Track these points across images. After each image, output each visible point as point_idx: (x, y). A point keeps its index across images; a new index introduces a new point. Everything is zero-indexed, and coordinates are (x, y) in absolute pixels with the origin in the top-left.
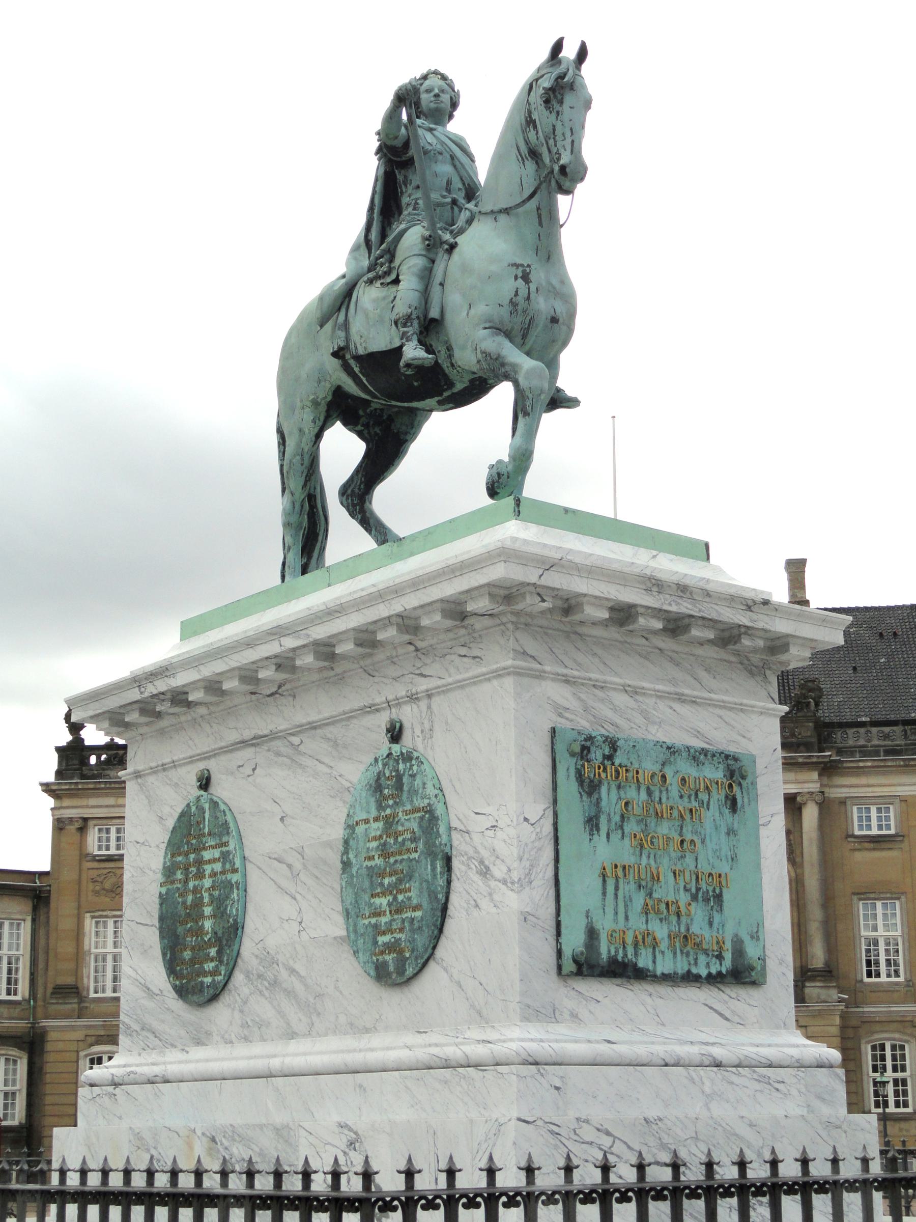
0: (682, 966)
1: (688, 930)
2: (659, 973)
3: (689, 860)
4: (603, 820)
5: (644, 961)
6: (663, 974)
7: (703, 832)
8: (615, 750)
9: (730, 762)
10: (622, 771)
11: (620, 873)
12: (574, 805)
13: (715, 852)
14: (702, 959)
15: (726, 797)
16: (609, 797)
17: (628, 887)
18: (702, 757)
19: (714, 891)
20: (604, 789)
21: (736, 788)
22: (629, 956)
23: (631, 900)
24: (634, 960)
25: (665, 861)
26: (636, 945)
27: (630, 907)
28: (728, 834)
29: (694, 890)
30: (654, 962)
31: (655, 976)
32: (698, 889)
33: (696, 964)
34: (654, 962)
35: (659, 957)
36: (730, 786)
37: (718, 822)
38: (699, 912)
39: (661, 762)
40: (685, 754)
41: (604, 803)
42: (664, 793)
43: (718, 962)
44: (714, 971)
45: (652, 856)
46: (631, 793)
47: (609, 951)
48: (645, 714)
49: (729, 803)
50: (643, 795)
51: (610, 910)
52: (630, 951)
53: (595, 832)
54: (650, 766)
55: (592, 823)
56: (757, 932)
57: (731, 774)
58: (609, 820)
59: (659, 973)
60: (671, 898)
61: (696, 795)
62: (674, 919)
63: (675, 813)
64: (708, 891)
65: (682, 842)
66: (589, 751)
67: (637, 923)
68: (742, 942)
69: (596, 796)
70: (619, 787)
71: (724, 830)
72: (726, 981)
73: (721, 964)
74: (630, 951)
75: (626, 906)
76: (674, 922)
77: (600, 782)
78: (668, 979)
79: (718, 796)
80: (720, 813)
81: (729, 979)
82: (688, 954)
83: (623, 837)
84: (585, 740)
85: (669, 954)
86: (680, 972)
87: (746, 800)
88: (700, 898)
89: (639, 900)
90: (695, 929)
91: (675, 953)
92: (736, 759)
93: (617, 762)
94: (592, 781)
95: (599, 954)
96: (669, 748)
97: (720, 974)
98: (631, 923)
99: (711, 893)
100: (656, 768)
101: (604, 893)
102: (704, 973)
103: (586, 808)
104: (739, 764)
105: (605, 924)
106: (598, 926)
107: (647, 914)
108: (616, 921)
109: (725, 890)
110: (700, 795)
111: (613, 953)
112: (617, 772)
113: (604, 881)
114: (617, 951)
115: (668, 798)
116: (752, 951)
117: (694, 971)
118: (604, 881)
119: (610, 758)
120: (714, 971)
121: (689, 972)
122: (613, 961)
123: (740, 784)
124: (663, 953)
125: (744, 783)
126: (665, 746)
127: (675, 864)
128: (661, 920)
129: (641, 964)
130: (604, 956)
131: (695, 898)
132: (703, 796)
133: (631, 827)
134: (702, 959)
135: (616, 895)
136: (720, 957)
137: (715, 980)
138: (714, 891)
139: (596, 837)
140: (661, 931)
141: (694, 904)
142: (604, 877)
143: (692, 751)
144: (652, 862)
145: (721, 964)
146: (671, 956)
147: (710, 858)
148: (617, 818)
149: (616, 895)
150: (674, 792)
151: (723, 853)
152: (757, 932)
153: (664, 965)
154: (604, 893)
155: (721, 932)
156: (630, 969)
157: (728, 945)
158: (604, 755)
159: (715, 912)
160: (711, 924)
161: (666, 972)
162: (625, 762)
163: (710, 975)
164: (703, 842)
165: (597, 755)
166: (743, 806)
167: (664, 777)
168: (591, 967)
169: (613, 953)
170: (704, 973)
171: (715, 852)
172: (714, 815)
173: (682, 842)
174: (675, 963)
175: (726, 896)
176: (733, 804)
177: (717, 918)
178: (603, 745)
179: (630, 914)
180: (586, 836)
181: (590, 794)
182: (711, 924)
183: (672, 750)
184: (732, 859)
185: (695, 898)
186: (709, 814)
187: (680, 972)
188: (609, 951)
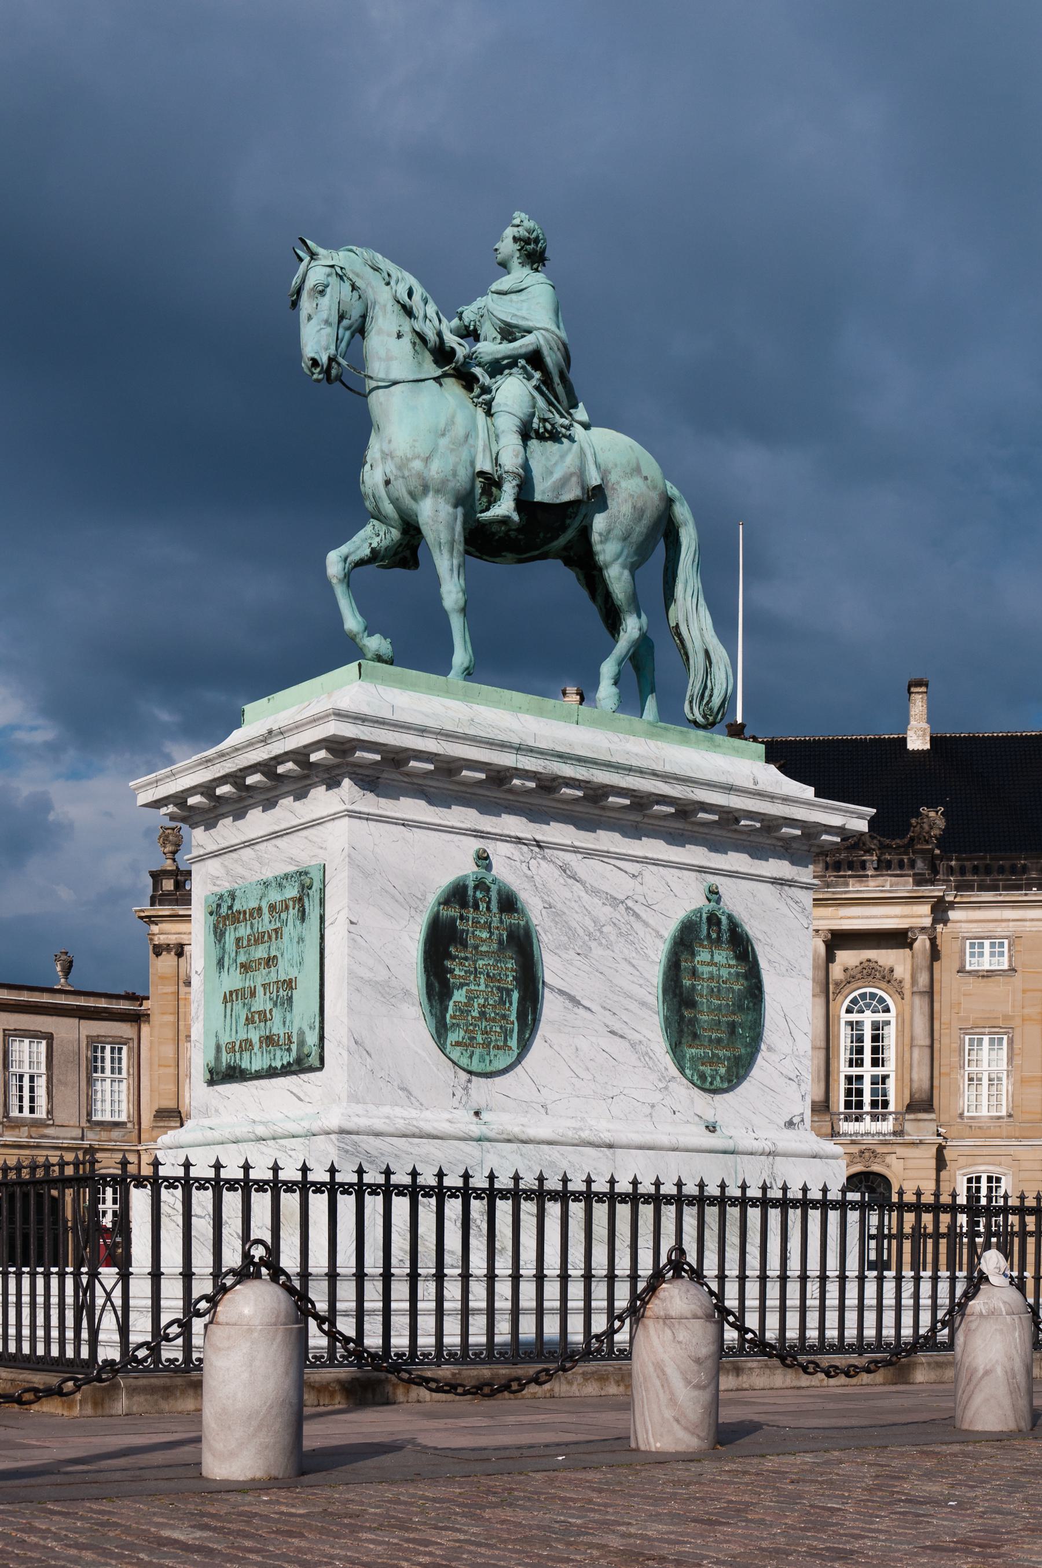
3: (273, 975)
14: (279, 1053)
21: (306, 900)
32: (277, 996)
40: (274, 885)
44: (285, 1063)
48: (259, 860)
57: (305, 888)
97: (289, 1063)
102: (279, 1065)
134: (279, 1053)
136: (289, 1050)
137: (286, 1071)
160: (284, 1023)
167: (260, 909)
170: (279, 1065)
182: (284, 1023)
183: (266, 884)
185: (275, 1005)
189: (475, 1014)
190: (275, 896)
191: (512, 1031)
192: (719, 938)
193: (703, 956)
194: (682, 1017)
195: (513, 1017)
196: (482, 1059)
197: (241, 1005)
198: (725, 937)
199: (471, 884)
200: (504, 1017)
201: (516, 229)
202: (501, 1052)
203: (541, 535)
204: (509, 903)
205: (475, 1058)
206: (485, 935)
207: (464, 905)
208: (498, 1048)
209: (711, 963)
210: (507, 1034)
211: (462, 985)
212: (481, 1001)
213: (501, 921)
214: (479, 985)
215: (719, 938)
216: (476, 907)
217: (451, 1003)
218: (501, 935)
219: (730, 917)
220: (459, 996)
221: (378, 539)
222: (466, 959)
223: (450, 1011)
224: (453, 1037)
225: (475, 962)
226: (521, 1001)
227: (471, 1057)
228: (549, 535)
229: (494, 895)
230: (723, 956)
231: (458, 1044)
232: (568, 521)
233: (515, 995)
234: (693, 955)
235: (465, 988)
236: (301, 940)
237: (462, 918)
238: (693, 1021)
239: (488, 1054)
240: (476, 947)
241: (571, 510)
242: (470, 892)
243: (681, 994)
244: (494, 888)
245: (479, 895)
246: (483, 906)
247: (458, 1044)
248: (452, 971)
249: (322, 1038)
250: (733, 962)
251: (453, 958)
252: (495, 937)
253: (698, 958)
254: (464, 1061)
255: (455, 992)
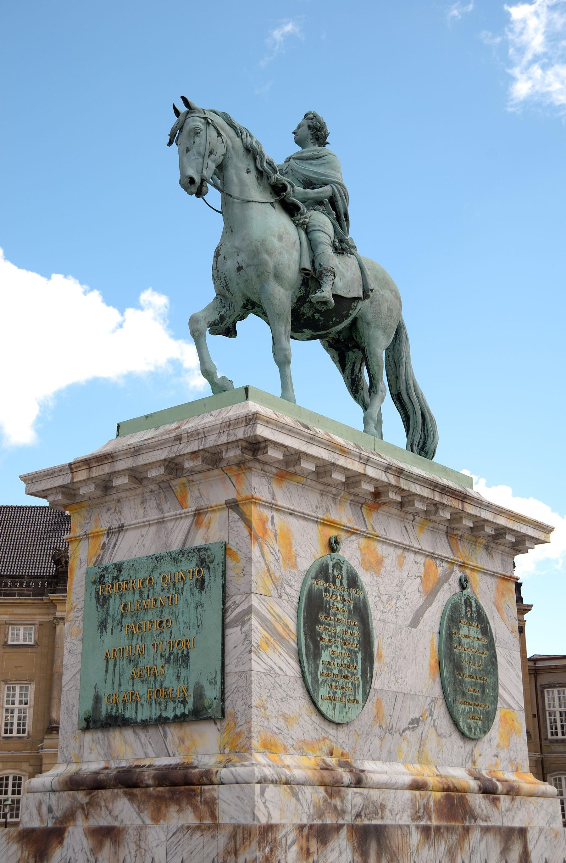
0: (155, 713)
1: (162, 685)
2: (139, 720)
3: (166, 635)
4: (110, 621)
5: (129, 713)
6: (142, 720)
7: (177, 612)
8: (121, 571)
9: (201, 553)
10: (124, 585)
11: (118, 655)
12: (95, 616)
13: (185, 623)
14: (171, 705)
15: (197, 580)
16: (115, 606)
17: (122, 663)
18: (181, 556)
19: (183, 653)
20: (112, 600)
22: (120, 711)
23: (124, 672)
24: (123, 713)
25: (148, 640)
26: (124, 702)
27: (122, 677)
28: (196, 608)
29: (167, 655)
30: (136, 713)
31: (136, 723)
32: (170, 654)
33: (166, 709)
34: (136, 713)
35: (140, 708)
36: (199, 571)
37: (189, 601)
38: (170, 671)
39: (150, 569)
41: (111, 610)
42: (151, 591)
43: (182, 706)
44: (179, 713)
45: (140, 638)
46: (129, 598)
47: (107, 709)
49: (198, 584)
50: (137, 596)
51: (109, 682)
52: (121, 706)
53: (104, 630)
54: (143, 575)
55: (103, 625)
56: (215, 678)
57: (202, 562)
58: (113, 621)
59: (139, 720)
60: (151, 665)
61: (174, 585)
62: (152, 679)
63: (158, 603)
64: (178, 654)
65: (161, 622)
66: (104, 578)
67: (127, 687)
68: (202, 687)
69: (106, 606)
70: (121, 596)
71: (193, 605)
72: (188, 719)
73: (185, 707)
74: (121, 706)
75: (120, 676)
76: (152, 682)
77: (110, 596)
78: (145, 724)
79: (190, 581)
80: (191, 593)
81: (191, 717)
82: (160, 704)
83: (121, 630)
84: (103, 571)
85: (147, 706)
86: (154, 717)
87: (212, 578)
88: (172, 661)
89: (129, 670)
90: (166, 684)
91: (151, 704)
92: (206, 550)
93: (121, 580)
94: (105, 597)
95: (100, 712)
96: (157, 558)
97: (183, 714)
98: (122, 687)
99: (180, 655)
100: (146, 575)
101: (107, 671)
102: (171, 715)
103: (100, 616)
104: (209, 553)
105: (105, 691)
106: (101, 694)
107: (133, 679)
108: (113, 688)
109: (190, 651)
110: (177, 585)
111: (109, 711)
112: (119, 585)
113: (107, 662)
114: (112, 709)
115: (153, 594)
116: (211, 693)
117: (164, 715)
118: (107, 662)
119: (116, 578)
120: (179, 713)
121: (160, 716)
122: (109, 716)
123: (208, 567)
124: (143, 705)
125: (211, 566)
126: (154, 557)
127: (156, 640)
128: (143, 682)
129: (127, 716)
130: (104, 713)
131: (168, 661)
132: (179, 585)
133: (128, 621)
134: (171, 705)
135: (114, 670)
136: (184, 702)
138: (183, 653)
139: (104, 633)
140: (142, 689)
141: (167, 666)
142: (107, 658)
143: (173, 554)
144: (140, 642)
145: (185, 707)
146: (149, 706)
147: (182, 630)
148: (119, 617)
149: (114, 670)
150: (158, 588)
151: (191, 623)
152: (215, 678)
153: (143, 714)
154: (107, 671)
155: (186, 683)
156: (119, 720)
157: (191, 692)
158: (113, 577)
159: (182, 669)
160: (178, 678)
161: (144, 718)
162: (127, 577)
163: (176, 716)
164: (177, 618)
165: (109, 579)
166: (209, 584)
168: (95, 722)
169: (109, 711)
170: (171, 715)
171: (185, 623)
172: (187, 596)
173: (161, 622)
174: (151, 711)
175: (192, 655)
176: (202, 584)
177: (183, 672)
178: (113, 571)
179: (122, 682)
180: (99, 634)
181: (102, 606)
182: (178, 678)
184: (198, 626)
185: (168, 661)
186: (183, 597)
187: (154, 717)
188: (107, 709)
189: (336, 672)
190: (168, 568)
191: (358, 687)
192: (472, 616)
193: (464, 631)
194: (455, 678)
195: (359, 675)
196: (341, 712)
197: (125, 661)
198: (475, 616)
199: (331, 564)
200: (353, 674)
201: (310, 121)
202: (351, 705)
203: (334, 319)
204: (353, 582)
205: (337, 709)
206: (340, 606)
207: (327, 580)
208: (350, 701)
209: (469, 637)
210: (355, 688)
211: (328, 647)
212: (339, 661)
213: (349, 595)
214: (337, 647)
215: (472, 616)
216: (334, 583)
217: (321, 663)
218: (349, 606)
219: (476, 602)
220: (325, 656)
221: (225, 309)
222: (329, 625)
223: (321, 669)
224: (324, 691)
225: (335, 627)
226: (364, 660)
227: (334, 709)
228: (338, 320)
229: (344, 572)
230: (474, 631)
231: (325, 698)
232: (351, 312)
233: (360, 656)
234: (458, 629)
235: (329, 649)
236: (199, 605)
237: (326, 591)
238: (462, 682)
239: (345, 707)
240: (335, 616)
241: (353, 304)
242: (330, 570)
243: (454, 659)
244: (344, 568)
245: (336, 573)
246: (338, 582)
247: (325, 698)
248: (320, 635)
249: (223, 692)
250: (480, 636)
251: (322, 624)
252: (346, 608)
253: (461, 632)
254: (329, 714)
255: (323, 652)
